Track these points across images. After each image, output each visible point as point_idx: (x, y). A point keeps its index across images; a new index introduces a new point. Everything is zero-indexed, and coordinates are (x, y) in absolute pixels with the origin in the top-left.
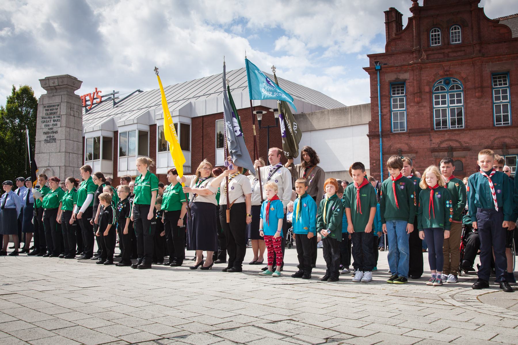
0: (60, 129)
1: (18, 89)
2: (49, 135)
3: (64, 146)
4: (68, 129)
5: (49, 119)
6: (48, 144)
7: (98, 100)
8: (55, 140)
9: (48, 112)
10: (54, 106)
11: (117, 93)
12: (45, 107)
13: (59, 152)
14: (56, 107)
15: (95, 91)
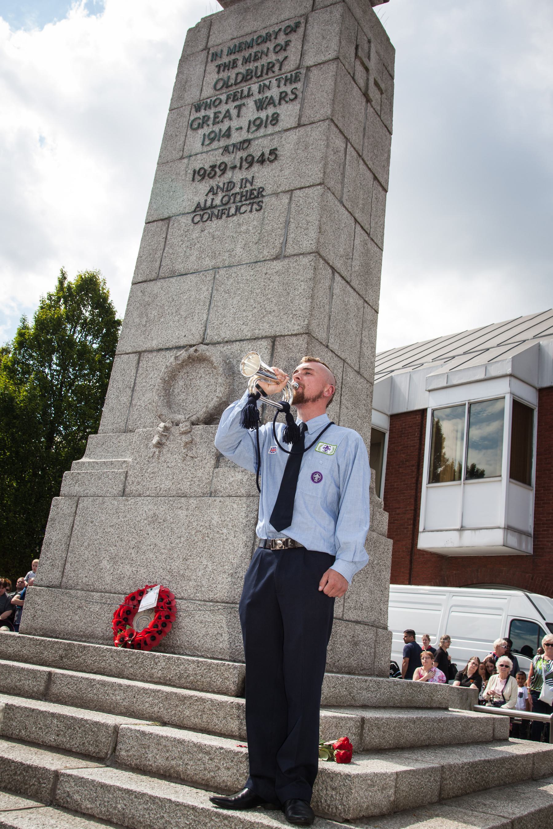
0: (293, 136)
1: (72, 279)
2: (220, 181)
3: (314, 218)
4: (339, 143)
5: (231, 106)
6: (214, 225)
8: (254, 198)
9: (232, 74)
10: (267, 38)
12: (215, 56)
13: (277, 258)
14: (282, 39)
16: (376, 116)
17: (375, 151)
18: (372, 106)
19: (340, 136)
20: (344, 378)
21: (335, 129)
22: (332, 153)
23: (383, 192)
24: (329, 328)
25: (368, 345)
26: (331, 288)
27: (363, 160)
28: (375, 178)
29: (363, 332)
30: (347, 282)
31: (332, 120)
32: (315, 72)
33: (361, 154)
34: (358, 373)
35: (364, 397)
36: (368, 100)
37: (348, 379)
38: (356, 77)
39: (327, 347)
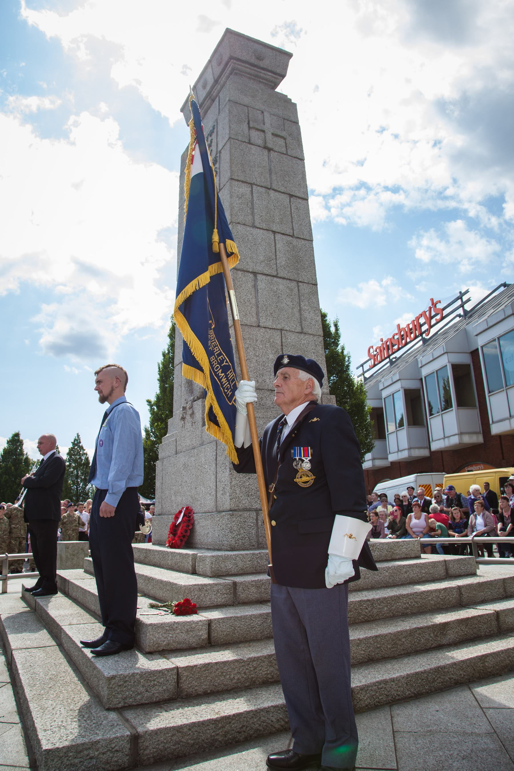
4: (245, 189)
7: (438, 317)
11: (467, 292)
15: (430, 305)
16: (282, 155)
17: (287, 179)
18: (275, 151)
19: (243, 184)
20: (284, 341)
21: (236, 183)
22: (237, 199)
23: (304, 202)
24: (257, 314)
25: (310, 310)
26: (255, 286)
27: (274, 190)
28: (291, 196)
29: (301, 303)
30: (273, 276)
31: (232, 179)
32: (223, 151)
33: (269, 187)
34: (301, 333)
35: (313, 347)
36: (269, 150)
37: (290, 340)
38: (252, 141)
39: (259, 326)
